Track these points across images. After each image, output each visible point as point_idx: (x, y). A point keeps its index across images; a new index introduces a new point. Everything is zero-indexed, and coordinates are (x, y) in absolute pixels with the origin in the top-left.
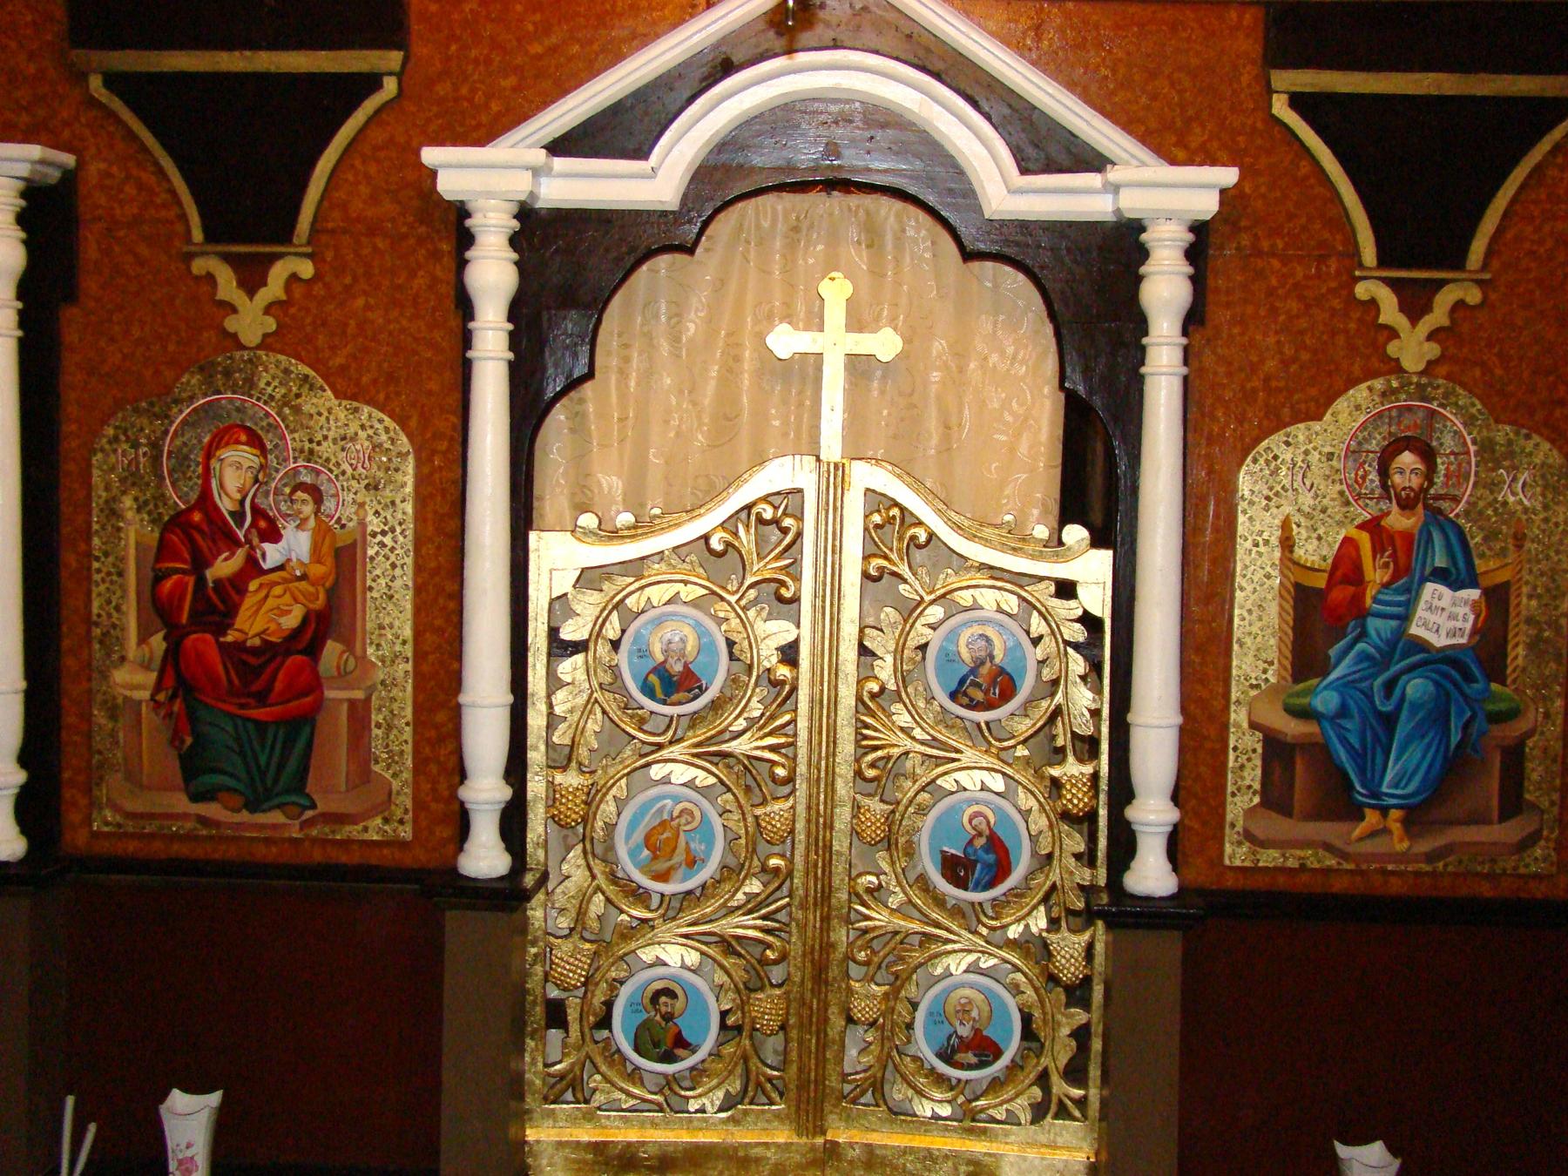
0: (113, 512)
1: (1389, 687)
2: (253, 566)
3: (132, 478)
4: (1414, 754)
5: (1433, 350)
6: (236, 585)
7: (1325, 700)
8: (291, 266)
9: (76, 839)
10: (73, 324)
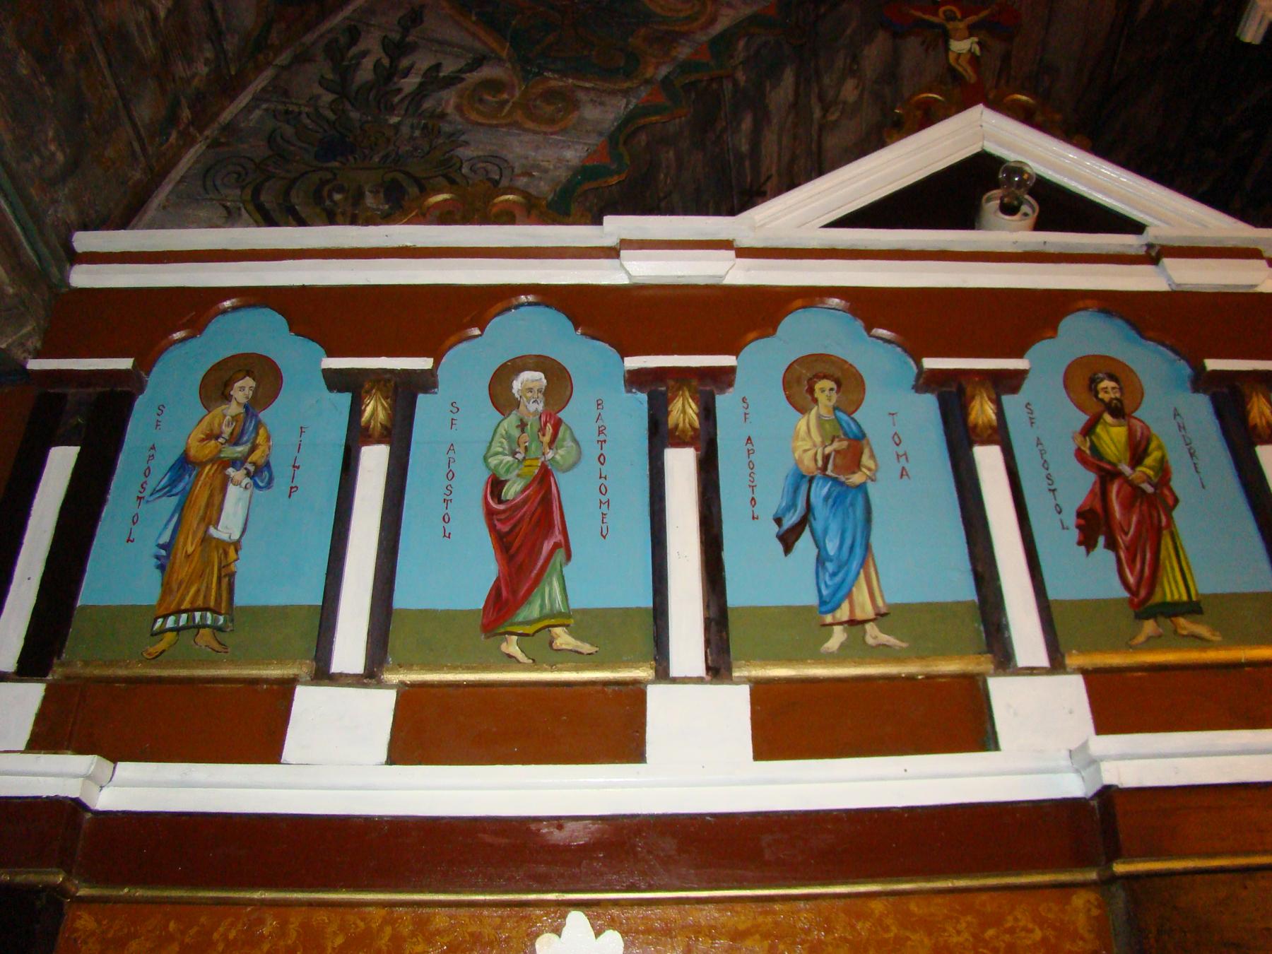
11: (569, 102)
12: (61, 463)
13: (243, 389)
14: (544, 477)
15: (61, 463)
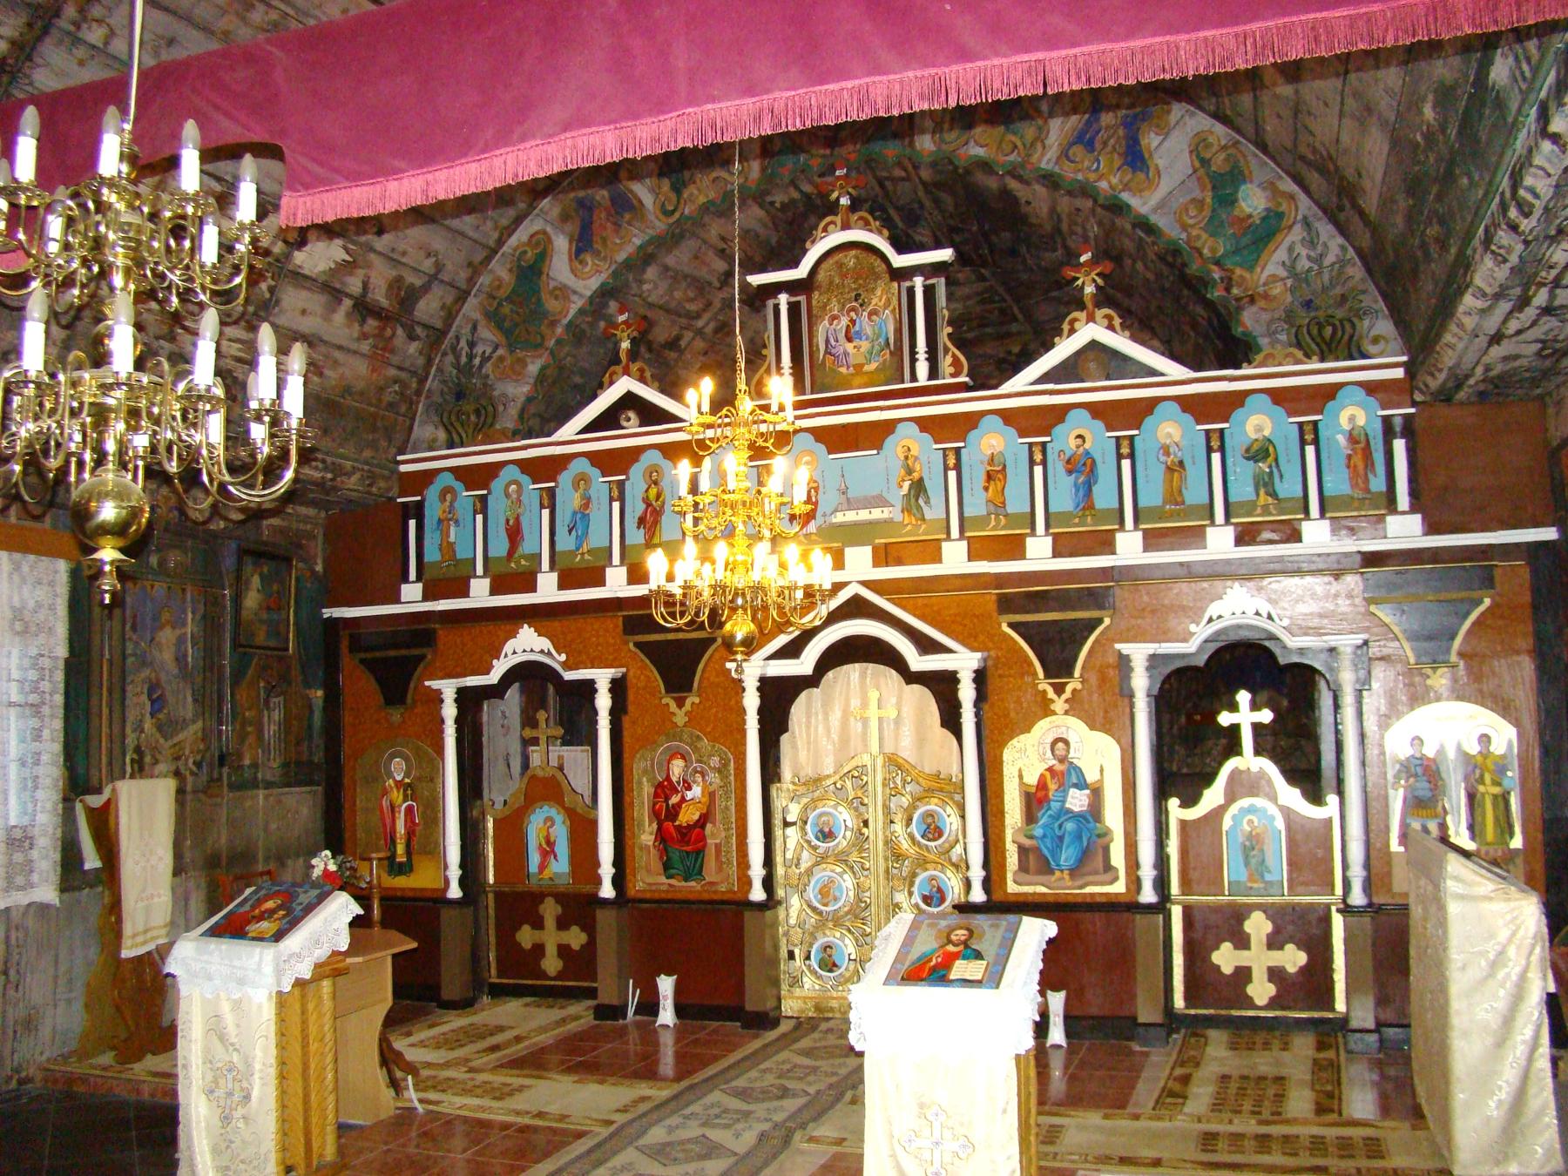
0: (640, 783)
1: (1060, 826)
2: (683, 800)
3: (645, 772)
4: (1071, 850)
5: (1067, 706)
6: (679, 805)
7: (1038, 832)
8: (692, 700)
9: (631, 893)
10: (626, 721)
11: (523, 363)
12: (412, 523)
13: (449, 497)
14: (517, 519)
15: (412, 523)
